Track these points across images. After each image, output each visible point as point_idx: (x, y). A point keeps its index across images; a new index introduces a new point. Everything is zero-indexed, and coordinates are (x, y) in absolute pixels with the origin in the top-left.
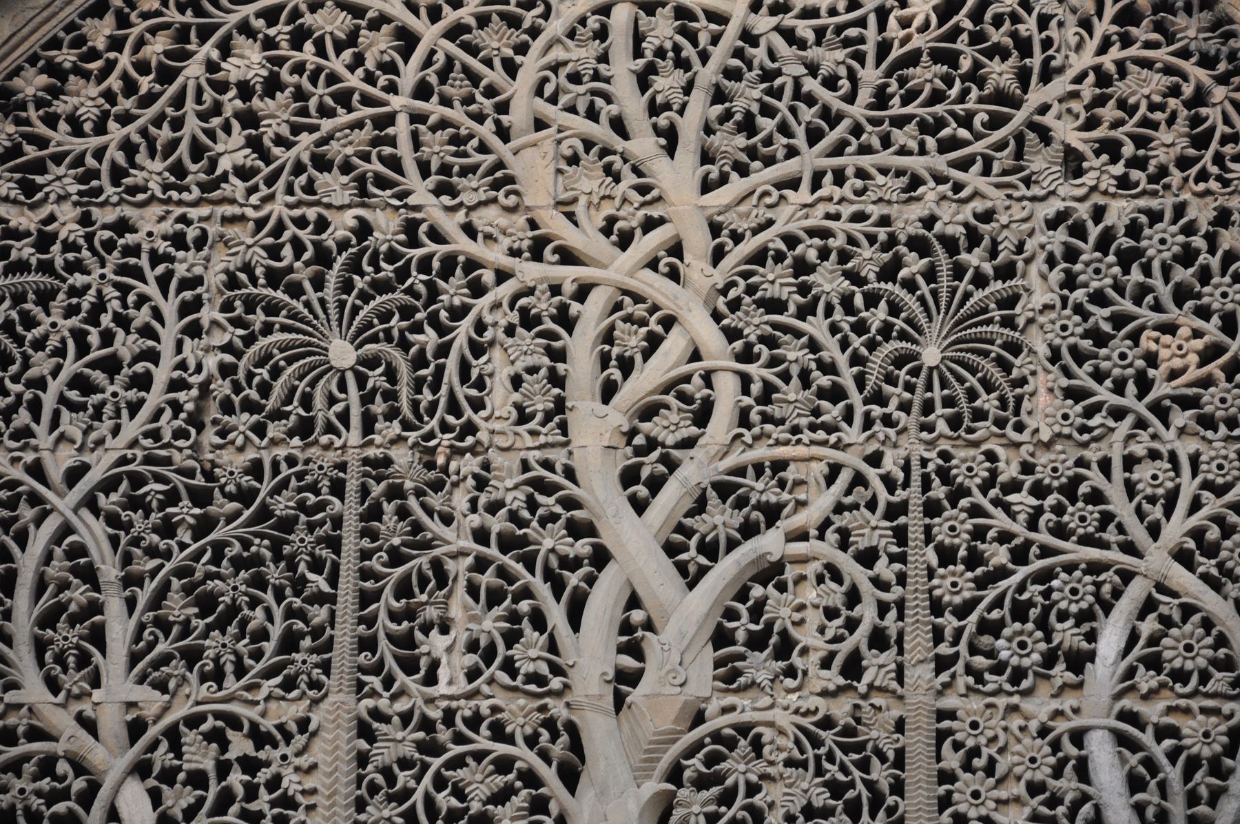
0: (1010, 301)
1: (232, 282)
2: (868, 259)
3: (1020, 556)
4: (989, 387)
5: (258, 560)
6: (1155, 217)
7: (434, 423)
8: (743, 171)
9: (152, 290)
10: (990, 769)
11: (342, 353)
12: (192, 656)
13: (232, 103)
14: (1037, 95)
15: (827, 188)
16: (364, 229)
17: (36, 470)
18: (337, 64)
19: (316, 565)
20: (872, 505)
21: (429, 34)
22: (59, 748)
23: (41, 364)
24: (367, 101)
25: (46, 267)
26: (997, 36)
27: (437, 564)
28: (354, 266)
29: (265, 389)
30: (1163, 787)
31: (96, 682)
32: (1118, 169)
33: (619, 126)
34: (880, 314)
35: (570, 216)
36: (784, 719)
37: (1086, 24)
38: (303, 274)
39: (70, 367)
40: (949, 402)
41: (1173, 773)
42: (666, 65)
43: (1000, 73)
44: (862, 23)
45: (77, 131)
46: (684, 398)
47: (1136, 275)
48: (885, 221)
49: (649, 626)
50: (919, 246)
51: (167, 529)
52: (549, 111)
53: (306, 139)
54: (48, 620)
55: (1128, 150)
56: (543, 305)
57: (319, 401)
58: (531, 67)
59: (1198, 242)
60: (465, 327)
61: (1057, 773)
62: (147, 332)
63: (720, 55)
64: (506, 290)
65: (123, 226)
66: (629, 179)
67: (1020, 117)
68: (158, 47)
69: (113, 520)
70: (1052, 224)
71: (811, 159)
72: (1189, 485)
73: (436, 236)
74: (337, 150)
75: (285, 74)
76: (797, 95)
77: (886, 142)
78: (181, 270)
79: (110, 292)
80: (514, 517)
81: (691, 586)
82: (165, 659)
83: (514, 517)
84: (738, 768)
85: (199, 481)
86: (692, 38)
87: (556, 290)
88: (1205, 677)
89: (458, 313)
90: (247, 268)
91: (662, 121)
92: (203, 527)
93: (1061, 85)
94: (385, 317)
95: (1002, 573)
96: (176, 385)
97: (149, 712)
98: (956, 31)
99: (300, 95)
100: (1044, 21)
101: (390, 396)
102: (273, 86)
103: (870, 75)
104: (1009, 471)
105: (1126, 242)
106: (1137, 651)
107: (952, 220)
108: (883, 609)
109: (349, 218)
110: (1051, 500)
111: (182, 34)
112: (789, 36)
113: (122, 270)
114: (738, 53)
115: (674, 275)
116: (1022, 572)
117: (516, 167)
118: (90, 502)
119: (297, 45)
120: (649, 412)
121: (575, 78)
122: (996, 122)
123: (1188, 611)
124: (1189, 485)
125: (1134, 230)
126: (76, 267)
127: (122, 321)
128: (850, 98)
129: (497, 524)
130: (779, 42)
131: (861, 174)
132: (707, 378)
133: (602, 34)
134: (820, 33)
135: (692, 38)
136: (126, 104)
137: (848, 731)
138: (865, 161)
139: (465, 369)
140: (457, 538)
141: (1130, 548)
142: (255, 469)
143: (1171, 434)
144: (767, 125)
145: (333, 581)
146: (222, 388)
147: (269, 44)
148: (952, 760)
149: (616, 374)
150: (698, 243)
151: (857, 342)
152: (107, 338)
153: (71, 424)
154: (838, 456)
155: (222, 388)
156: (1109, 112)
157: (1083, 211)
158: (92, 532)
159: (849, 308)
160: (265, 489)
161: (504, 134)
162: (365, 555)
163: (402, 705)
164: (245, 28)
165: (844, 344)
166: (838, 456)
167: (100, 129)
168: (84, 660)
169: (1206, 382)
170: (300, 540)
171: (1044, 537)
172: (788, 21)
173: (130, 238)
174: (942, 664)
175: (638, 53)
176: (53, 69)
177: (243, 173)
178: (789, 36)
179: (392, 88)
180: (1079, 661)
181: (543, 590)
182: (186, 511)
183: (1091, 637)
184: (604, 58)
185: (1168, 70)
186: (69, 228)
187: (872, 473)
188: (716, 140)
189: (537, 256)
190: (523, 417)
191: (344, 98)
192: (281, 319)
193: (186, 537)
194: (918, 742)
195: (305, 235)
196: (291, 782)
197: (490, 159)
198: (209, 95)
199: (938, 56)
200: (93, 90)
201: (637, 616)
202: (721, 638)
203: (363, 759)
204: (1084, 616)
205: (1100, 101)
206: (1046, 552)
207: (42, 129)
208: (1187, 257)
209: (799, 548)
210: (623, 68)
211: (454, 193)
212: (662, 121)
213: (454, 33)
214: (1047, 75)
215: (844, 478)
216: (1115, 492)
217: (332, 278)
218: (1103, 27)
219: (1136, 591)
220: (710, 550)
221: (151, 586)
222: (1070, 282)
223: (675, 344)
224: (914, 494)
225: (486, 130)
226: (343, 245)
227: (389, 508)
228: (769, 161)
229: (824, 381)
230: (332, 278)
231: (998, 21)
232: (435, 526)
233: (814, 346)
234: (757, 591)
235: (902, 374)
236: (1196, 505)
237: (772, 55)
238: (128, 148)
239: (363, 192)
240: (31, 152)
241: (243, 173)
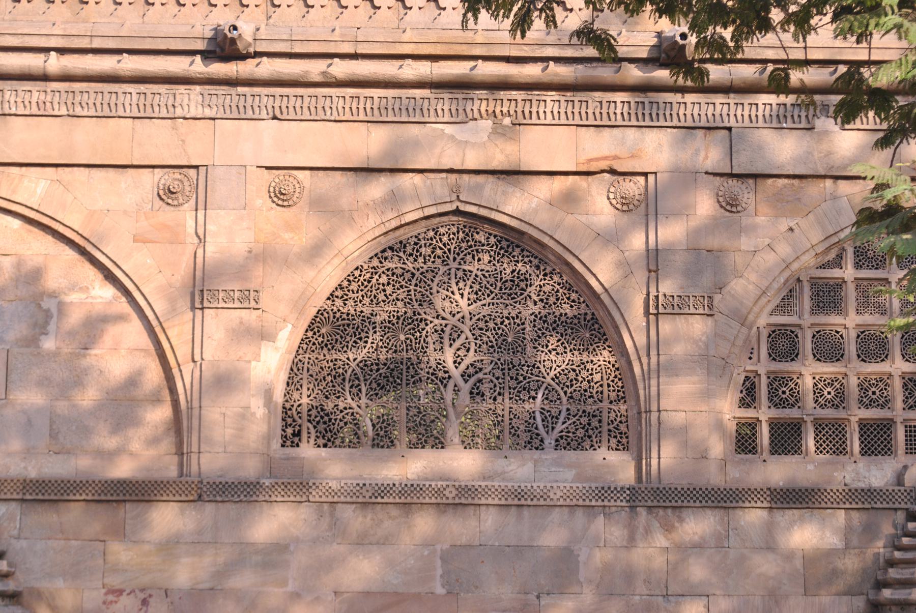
0: (524, 329)
1: (382, 323)
2: (499, 320)
3: (525, 378)
4: (520, 346)
5: (388, 377)
6: (549, 314)
7: (419, 351)
8: (475, 302)
9: (367, 324)
10: (518, 418)
11: (402, 337)
12: (377, 394)
13: (381, 287)
14: (529, 289)
15: (491, 306)
16: (405, 313)
17: (348, 359)
18: (400, 280)
19: (398, 378)
20: (499, 368)
21: (417, 274)
22: (355, 411)
23: (348, 338)
24: (406, 287)
25: (348, 319)
26: (522, 278)
27: (420, 378)
28: (404, 320)
29: (388, 344)
30: (548, 421)
31: (360, 399)
32: (543, 304)
33: (453, 293)
34: (500, 332)
35: (444, 311)
36: (483, 409)
37: (538, 276)
38: (395, 321)
39: (354, 339)
40: (512, 349)
41: (549, 419)
42: (461, 281)
43: (523, 285)
44: (497, 274)
45: (353, 293)
46: (465, 347)
47: (546, 325)
48: (501, 313)
49: (458, 390)
50: (508, 318)
51: (371, 370)
52: (440, 290)
53: (395, 295)
54: (351, 387)
55: (545, 301)
56: (439, 328)
57: (398, 346)
58: (436, 280)
59: (557, 319)
60: (424, 332)
61: (530, 419)
62: (367, 332)
63: (471, 279)
64: (432, 325)
65: (362, 312)
66: (455, 303)
67: (526, 294)
68: (368, 275)
69: (362, 368)
70: (531, 315)
71: (488, 300)
72: (554, 366)
73: (419, 314)
74: (400, 297)
75: (391, 281)
76: (485, 287)
77: (502, 297)
78: (373, 320)
79: (360, 325)
80: (434, 370)
81: (466, 382)
82: (372, 395)
83: (434, 370)
85: (377, 361)
86: (466, 275)
87: (441, 325)
88: (555, 401)
89: (423, 329)
90: (384, 320)
91: (461, 292)
92: (378, 370)
93: (533, 287)
94: (410, 330)
95: (521, 382)
96: (372, 343)
97: (370, 405)
98: (514, 276)
99: (394, 286)
100: (530, 275)
101: (411, 345)
102: (389, 284)
103: (499, 284)
104: (523, 362)
105: (544, 319)
106: (545, 396)
107: (513, 314)
108: (500, 388)
109: (403, 310)
110: (530, 368)
111: (372, 274)
112: (484, 275)
113: (362, 320)
114: (474, 279)
115: (463, 323)
116: (525, 382)
117: (434, 301)
118: (358, 365)
119: (393, 276)
120: (458, 349)
121: (444, 283)
122: (522, 294)
123: (553, 389)
124: (554, 366)
125: (546, 316)
126: (354, 319)
127: (362, 330)
128: (495, 289)
129: (431, 371)
130: (482, 277)
131: (497, 304)
132: (469, 343)
133: (449, 274)
134: (490, 275)
135: (466, 275)
136: (362, 288)
137: (494, 411)
138: (498, 301)
139: (424, 340)
141: (544, 377)
142: (387, 359)
143: (551, 356)
144: (480, 293)
145: (401, 381)
146: (380, 344)
147: (388, 275)
148: (512, 416)
149: (452, 342)
150: (468, 316)
151: (496, 337)
152: (360, 333)
153: (354, 350)
154: (493, 359)
155: (380, 344)
156: (542, 293)
157: (537, 313)
158: (358, 371)
159: (495, 330)
160: (389, 363)
161: (431, 294)
162: (407, 376)
163: (414, 405)
164: (383, 272)
165: (494, 337)
166: (493, 359)
167: (357, 292)
168: (358, 395)
169: (558, 346)
170: (395, 373)
171: (529, 375)
172: (484, 272)
173: (363, 314)
174: (511, 399)
175: (456, 278)
176: (349, 281)
177: (384, 301)
178: (484, 275)
179: (410, 285)
180: (534, 398)
181: (439, 383)
182: (375, 367)
183: (536, 394)
184: (449, 279)
185: (552, 285)
186: (352, 312)
187: (499, 362)
188: (470, 296)
189: (437, 318)
190: (435, 350)
191: (401, 286)
192: (391, 330)
193: (374, 372)
194: (506, 413)
195: (395, 314)
196: (395, 419)
197: (428, 299)
198: (377, 286)
199: (511, 281)
200: (356, 285)
201: (456, 389)
202: (471, 393)
203: (407, 414)
204: (536, 390)
205: (540, 291)
206: (529, 378)
207: (347, 293)
208: (555, 322)
209: (486, 376)
210: (453, 281)
211: (422, 305)
212: (461, 292)
213: (422, 274)
214: (531, 285)
215: (494, 363)
216: (542, 367)
217: (401, 322)
218: (541, 277)
219: (545, 385)
220: (469, 376)
221: (369, 381)
222: (534, 326)
223: (463, 336)
224: (506, 367)
225: (428, 293)
226: (402, 316)
227: (411, 367)
228: (480, 300)
229: (490, 344)
230: (401, 322)
231: (522, 274)
232: (419, 371)
233: (488, 337)
234: (478, 384)
235: (504, 343)
236: (555, 369)
237: (481, 279)
238: (363, 296)
239: (405, 305)
240: (345, 297)
241: (384, 301)
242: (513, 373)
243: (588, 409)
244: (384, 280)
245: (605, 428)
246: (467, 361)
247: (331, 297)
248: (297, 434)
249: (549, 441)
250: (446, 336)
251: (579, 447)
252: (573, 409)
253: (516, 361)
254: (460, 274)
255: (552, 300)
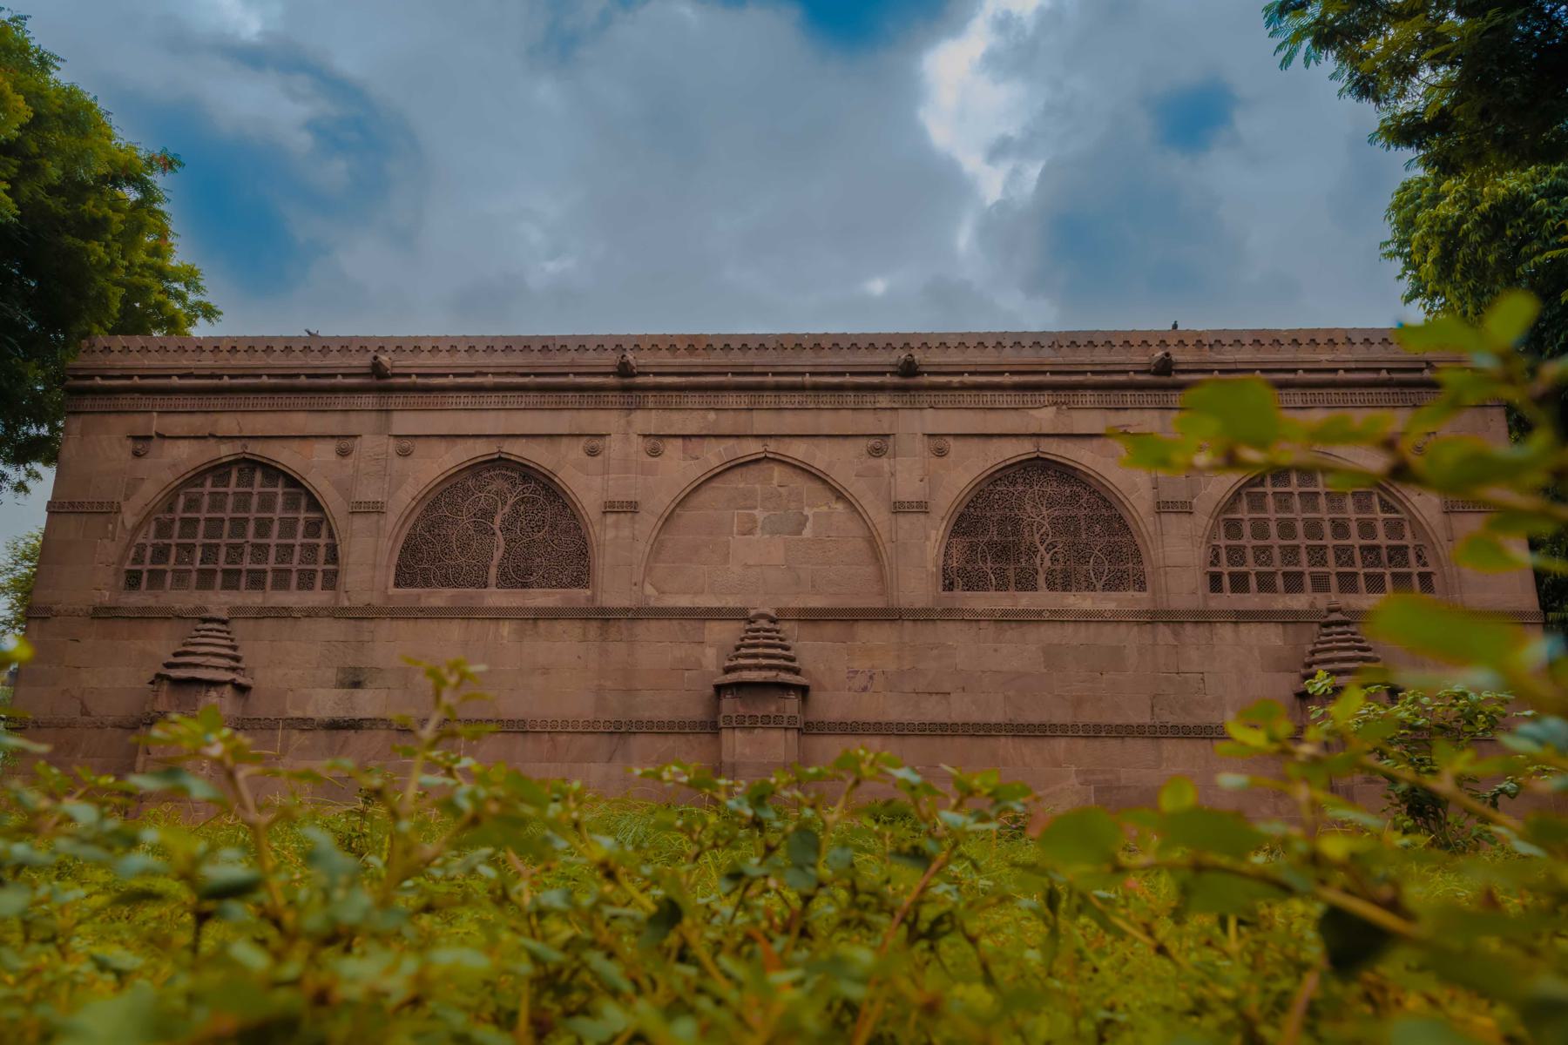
84: (1054, 573)
140: (1022, 549)
242: (1075, 548)
243: (1121, 568)
244: (997, 497)
245: (1131, 579)
246: (1047, 542)
247: (968, 506)
248: (952, 583)
249: (1099, 586)
250: (1035, 528)
251: (1117, 589)
252: (1112, 568)
253: (1076, 541)
254: (1041, 493)
255: (1095, 507)
